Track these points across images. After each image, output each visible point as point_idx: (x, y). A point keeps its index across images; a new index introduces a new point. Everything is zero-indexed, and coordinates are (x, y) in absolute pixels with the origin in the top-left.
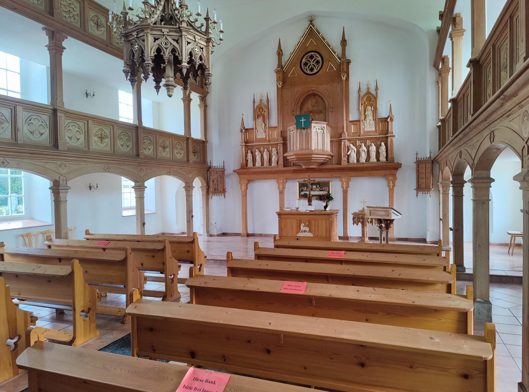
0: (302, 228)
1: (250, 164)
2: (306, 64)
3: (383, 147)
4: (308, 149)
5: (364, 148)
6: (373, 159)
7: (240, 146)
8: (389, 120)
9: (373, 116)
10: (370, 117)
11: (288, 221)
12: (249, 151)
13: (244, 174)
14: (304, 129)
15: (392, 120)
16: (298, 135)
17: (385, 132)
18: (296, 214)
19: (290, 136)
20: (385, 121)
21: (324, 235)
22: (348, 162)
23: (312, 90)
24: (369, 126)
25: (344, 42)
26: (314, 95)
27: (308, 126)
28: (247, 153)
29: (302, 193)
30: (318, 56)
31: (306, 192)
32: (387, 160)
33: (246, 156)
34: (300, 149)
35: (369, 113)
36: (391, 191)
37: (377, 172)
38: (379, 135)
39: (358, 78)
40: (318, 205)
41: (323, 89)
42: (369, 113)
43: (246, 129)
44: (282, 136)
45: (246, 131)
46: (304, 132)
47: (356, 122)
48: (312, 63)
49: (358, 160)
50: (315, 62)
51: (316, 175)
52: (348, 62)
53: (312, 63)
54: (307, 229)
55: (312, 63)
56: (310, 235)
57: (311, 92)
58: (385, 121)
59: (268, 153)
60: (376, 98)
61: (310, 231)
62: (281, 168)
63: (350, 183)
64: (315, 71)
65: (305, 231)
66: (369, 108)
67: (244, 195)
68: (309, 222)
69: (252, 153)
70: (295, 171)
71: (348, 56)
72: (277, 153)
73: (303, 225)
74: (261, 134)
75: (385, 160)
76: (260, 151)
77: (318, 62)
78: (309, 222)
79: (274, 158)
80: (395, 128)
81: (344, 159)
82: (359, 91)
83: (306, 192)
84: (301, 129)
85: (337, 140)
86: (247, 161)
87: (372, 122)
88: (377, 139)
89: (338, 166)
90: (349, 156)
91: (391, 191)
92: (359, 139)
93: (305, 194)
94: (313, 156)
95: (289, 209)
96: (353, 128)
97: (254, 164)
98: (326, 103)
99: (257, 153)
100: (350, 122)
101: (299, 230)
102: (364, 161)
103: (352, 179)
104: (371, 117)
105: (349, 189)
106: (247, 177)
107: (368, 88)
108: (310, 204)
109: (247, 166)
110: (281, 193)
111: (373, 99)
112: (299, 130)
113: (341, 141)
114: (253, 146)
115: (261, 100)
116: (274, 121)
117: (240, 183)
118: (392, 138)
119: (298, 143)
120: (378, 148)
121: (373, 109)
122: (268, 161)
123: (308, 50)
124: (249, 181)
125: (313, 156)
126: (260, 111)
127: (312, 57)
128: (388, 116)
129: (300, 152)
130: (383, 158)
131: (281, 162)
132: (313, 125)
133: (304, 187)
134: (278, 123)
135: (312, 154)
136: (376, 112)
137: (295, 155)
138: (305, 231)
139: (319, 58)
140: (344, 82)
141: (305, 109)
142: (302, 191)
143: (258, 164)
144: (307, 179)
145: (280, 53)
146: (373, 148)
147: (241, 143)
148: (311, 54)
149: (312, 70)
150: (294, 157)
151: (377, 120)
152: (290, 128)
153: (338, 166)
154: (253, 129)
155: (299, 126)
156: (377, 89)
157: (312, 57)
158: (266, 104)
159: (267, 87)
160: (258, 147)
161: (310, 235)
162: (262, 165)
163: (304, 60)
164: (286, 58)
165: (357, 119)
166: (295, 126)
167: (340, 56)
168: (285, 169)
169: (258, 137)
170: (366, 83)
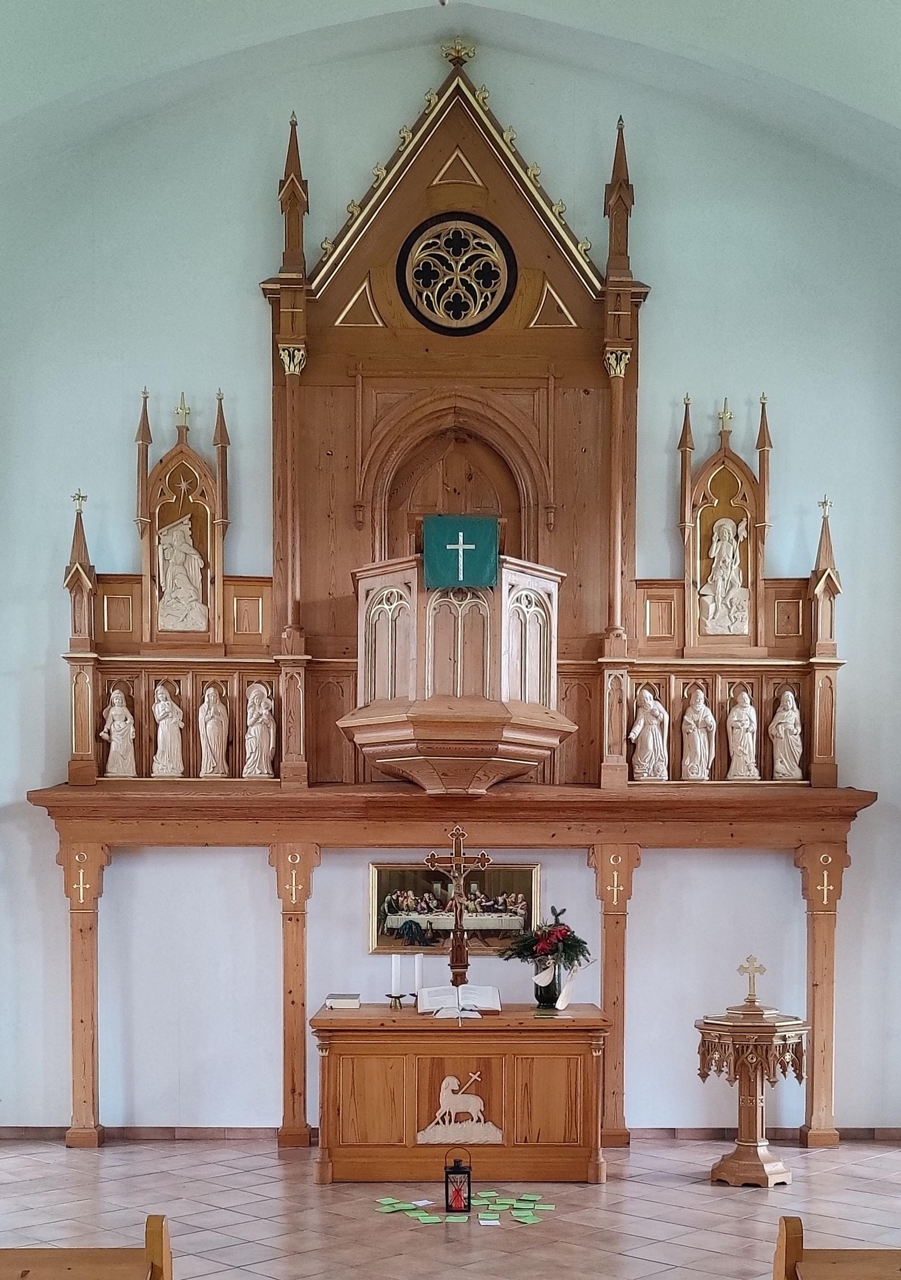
0: (449, 1101)
1: (122, 764)
2: (426, 275)
3: (791, 716)
4: (480, 697)
5: (703, 712)
6: (745, 766)
7: (66, 665)
8: (819, 589)
9: (744, 567)
10: (730, 572)
11: (373, 1065)
12: (116, 696)
13: (92, 813)
14: (460, 592)
15: (832, 590)
16: (430, 623)
17: (794, 644)
18: (400, 1028)
19: (372, 628)
20: (801, 593)
21: (558, 1134)
22: (631, 778)
23: (457, 411)
24: (726, 616)
25: (620, 195)
26: (463, 436)
27: (482, 583)
28: (103, 703)
29: (395, 921)
30: (491, 242)
31: (414, 916)
32: (806, 775)
33: (100, 722)
34: (439, 697)
35: (726, 550)
36: (821, 917)
37: (768, 826)
38: (770, 656)
39: (679, 378)
40: (497, 984)
41: (513, 409)
42: (726, 550)
43: (100, 579)
44: (299, 625)
45: (93, 586)
46: (462, 607)
47: (669, 589)
48: (457, 273)
49: (676, 770)
50: (473, 269)
51: (453, 832)
52: (639, 296)
53: (458, 275)
54: (474, 1105)
55: (458, 275)
56: (489, 1134)
57: (449, 421)
58: (801, 593)
59: (221, 709)
60: (758, 487)
61: (487, 1116)
62: (295, 789)
63: (636, 873)
64: (474, 316)
65: (461, 1117)
66: (728, 525)
67: (85, 930)
68: (485, 1067)
69: (130, 703)
70: (370, 811)
71: (642, 266)
72: (276, 715)
73: (450, 1083)
74: (181, 610)
75: (797, 773)
76: (176, 699)
77: (487, 275)
78: (485, 1067)
79: (257, 740)
80: (844, 628)
81: (613, 761)
82: (685, 442)
83: (414, 916)
84: (445, 594)
85: (584, 666)
86: (104, 746)
87: (740, 594)
88: (761, 674)
89: (590, 794)
90: (632, 747)
91: (821, 917)
92: (683, 672)
93: (410, 924)
94: (508, 734)
95: (353, 1004)
96: (651, 617)
97: (144, 767)
98: (525, 485)
99: (159, 709)
100: (641, 584)
101: (430, 1112)
102: (702, 774)
103: (648, 857)
104: (733, 573)
105: (310, 905)
106: (103, 828)
107: (724, 435)
108: (458, 980)
109: (102, 771)
110: (294, 917)
111: (744, 488)
112: (434, 600)
113: (599, 670)
114: (135, 670)
115: (183, 432)
116: (251, 547)
117: (63, 860)
118: (830, 673)
119: (429, 667)
120: (768, 712)
121: (743, 534)
122: (220, 752)
123: (441, 207)
124: (114, 851)
125: (508, 734)
126: (179, 489)
127: (457, 243)
128: (817, 575)
129: (441, 711)
130: (787, 766)
131: (295, 758)
132: (508, 576)
133: (404, 889)
134: (280, 559)
135: (505, 724)
136: (756, 551)
137: (414, 722)
138: (461, 1117)
139: (496, 256)
140: (619, 388)
141: (413, 505)
142: (395, 908)
143: (167, 763)
144: (445, 853)
145: (294, 198)
146: (746, 716)
147: (74, 645)
148: (453, 225)
149: (457, 307)
150: (408, 733)
151: (761, 585)
152: (376, 583)
153: (590, 794)
154: (136, 579)
155: (436, 579)
156: (763, 440)
157: (457, 243)
158: (213, 454)
159: (219, 366)
160: (168, 676)
161: (489, 1134)
162: (186, 774)
163: (417, 254)
164: (318, 229)
165: (665, 573)
166: (412, 576)
167: (602, 259)
168: (320, 794)
169: (168, 622)
170: (711, 412)
